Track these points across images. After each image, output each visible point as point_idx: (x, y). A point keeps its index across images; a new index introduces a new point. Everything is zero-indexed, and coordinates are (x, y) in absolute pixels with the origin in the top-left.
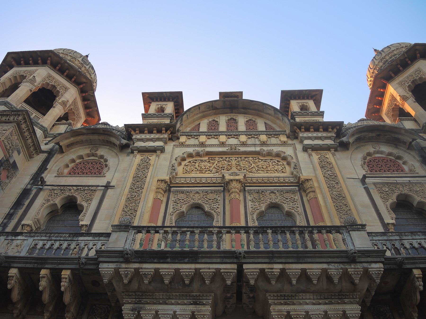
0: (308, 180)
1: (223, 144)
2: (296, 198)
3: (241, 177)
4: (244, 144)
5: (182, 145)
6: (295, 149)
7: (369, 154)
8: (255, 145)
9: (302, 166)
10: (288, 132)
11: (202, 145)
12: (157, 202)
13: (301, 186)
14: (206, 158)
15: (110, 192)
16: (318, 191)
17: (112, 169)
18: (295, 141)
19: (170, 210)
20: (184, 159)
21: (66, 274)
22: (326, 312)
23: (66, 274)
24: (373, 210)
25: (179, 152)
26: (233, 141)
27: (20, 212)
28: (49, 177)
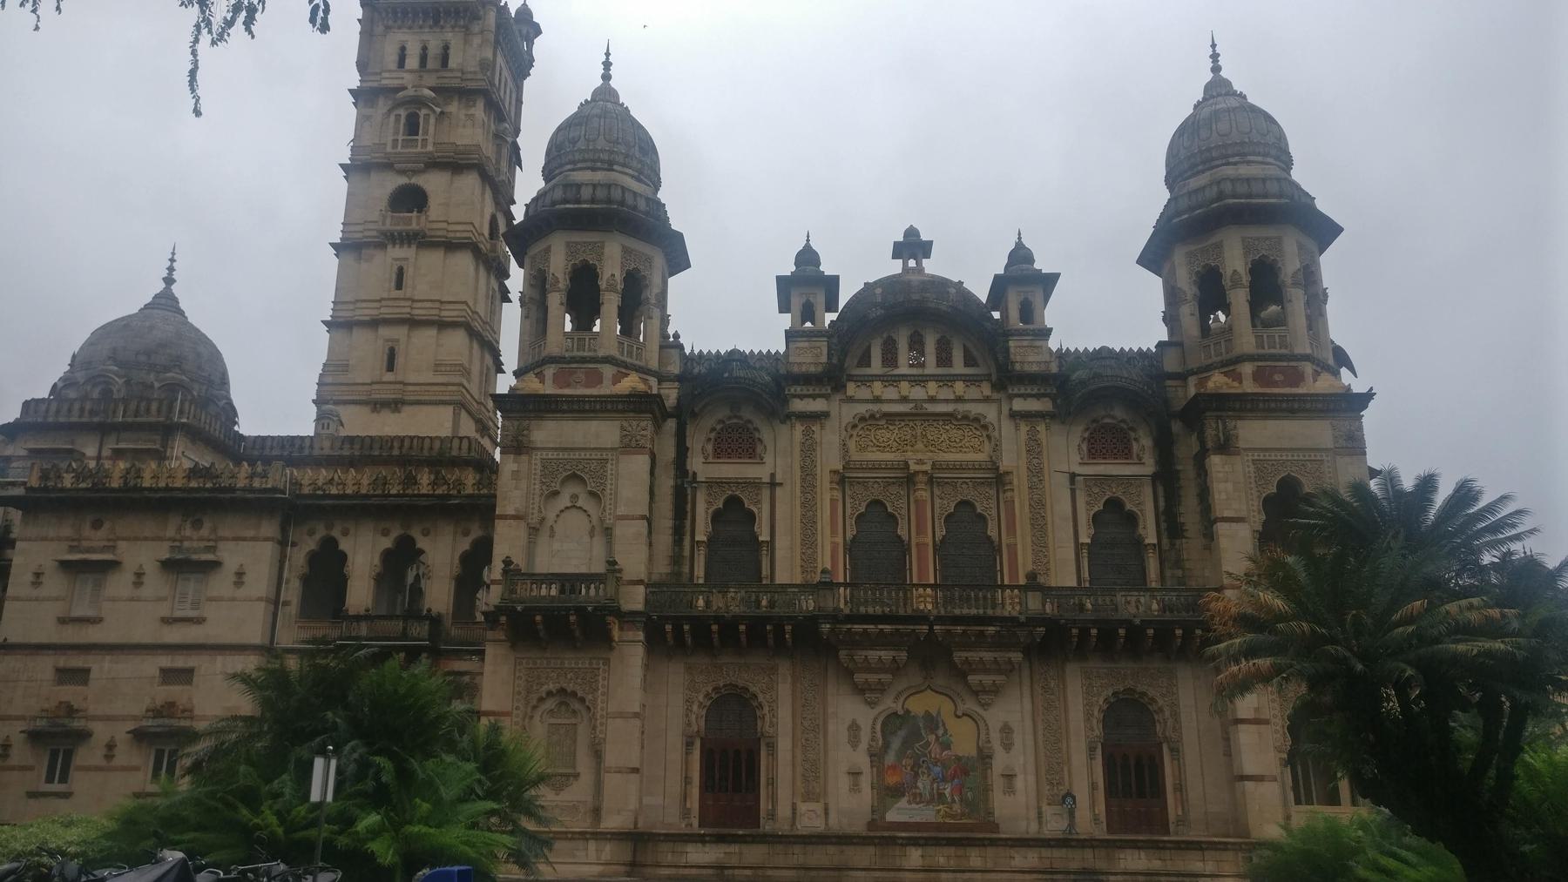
0: (1008, 473)
1: (904, 399)
3: (927, 467)
4: (932, 400)
5: (851, 400)
6: (1000, 412)
7: (1094, 421)
8: (947, 401)
9: (1004, 446)
10: (994, 378)
11: (877, 400)
13: (1000, 480)
14: (883, 422)
15: (778, 491)
17: (770, 448)
19: (848, 511)
20: (854, 426)
21: (788, 628)
23: (788, 628)
25: (849, 412)
26: (918, 393)
27: (688, 523)
28: (696, 464)
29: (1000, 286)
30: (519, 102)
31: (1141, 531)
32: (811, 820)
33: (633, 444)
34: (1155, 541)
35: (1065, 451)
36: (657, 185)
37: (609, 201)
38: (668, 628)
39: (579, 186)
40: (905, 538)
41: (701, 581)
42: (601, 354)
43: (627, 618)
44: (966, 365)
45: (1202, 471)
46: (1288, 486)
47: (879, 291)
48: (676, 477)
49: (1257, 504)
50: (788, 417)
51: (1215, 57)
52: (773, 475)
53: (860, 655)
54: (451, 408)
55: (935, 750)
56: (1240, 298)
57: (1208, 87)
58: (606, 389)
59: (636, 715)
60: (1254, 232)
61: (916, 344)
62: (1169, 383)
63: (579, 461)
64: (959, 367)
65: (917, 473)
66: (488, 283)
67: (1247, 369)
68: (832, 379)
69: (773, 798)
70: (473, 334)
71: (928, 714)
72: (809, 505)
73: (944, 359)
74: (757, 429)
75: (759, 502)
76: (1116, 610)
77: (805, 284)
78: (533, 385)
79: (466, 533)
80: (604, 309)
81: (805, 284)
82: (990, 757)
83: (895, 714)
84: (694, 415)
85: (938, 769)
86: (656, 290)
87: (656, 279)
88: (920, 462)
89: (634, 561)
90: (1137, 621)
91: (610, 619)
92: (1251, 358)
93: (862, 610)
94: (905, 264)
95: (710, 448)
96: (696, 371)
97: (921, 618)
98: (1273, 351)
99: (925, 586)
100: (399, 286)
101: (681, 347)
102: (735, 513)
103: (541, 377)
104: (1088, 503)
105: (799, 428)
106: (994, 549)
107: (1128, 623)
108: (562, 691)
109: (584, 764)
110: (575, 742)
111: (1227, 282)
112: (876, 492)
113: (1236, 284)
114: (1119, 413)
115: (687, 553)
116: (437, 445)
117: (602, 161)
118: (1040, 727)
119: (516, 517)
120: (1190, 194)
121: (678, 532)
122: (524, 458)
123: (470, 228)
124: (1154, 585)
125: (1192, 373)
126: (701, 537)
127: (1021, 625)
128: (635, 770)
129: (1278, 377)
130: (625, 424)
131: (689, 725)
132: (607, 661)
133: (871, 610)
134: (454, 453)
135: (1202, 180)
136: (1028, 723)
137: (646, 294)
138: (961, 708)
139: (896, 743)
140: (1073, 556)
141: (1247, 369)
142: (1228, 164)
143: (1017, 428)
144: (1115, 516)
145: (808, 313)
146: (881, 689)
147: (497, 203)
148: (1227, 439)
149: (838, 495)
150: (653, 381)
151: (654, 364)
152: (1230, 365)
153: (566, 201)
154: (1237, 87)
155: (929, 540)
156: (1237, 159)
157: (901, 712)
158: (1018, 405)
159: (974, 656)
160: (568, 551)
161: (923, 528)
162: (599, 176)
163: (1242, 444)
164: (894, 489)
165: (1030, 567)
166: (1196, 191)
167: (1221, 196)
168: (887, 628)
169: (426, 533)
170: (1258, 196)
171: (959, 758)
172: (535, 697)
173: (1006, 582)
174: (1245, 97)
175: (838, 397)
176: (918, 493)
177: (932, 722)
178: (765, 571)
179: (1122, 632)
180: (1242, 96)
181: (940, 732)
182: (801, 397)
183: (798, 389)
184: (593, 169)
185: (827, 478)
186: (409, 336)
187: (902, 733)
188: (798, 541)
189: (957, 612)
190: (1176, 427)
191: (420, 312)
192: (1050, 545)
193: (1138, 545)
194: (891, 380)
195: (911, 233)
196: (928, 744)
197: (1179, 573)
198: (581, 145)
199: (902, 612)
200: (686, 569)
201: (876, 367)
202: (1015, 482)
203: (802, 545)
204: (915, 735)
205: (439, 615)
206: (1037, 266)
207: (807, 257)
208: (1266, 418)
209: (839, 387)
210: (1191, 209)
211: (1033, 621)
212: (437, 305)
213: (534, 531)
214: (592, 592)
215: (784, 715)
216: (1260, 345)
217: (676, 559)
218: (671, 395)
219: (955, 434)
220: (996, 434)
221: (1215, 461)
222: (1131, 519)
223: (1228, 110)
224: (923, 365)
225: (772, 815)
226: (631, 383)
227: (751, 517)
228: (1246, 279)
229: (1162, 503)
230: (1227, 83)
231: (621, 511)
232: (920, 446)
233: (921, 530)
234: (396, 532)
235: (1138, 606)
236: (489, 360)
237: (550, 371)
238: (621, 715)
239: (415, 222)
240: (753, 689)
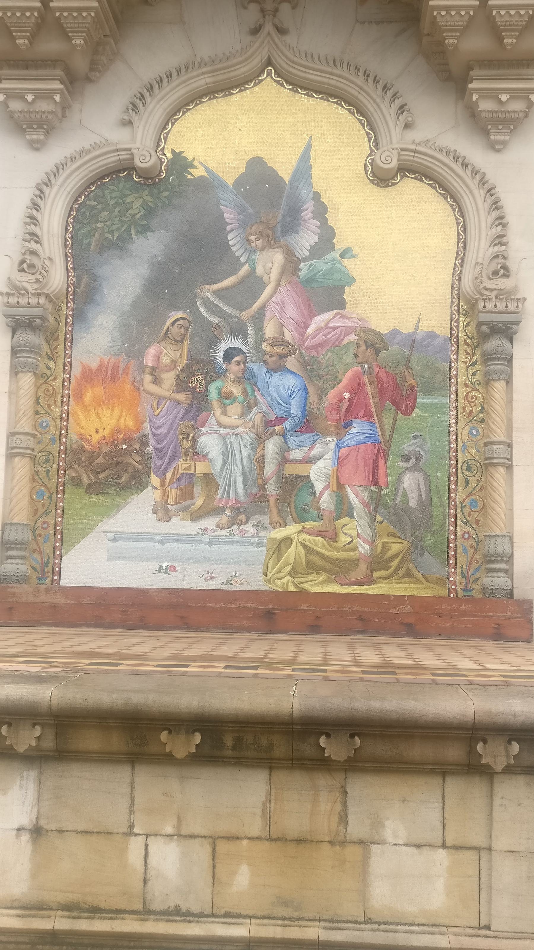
55: (280, 312)
71: (259, 178)
85: (284, 384)
139: (124, 281)
171: (373, 343)
181: (305, 240)
187: (150, 247)
196: (253, 285)
204: (200, 254)
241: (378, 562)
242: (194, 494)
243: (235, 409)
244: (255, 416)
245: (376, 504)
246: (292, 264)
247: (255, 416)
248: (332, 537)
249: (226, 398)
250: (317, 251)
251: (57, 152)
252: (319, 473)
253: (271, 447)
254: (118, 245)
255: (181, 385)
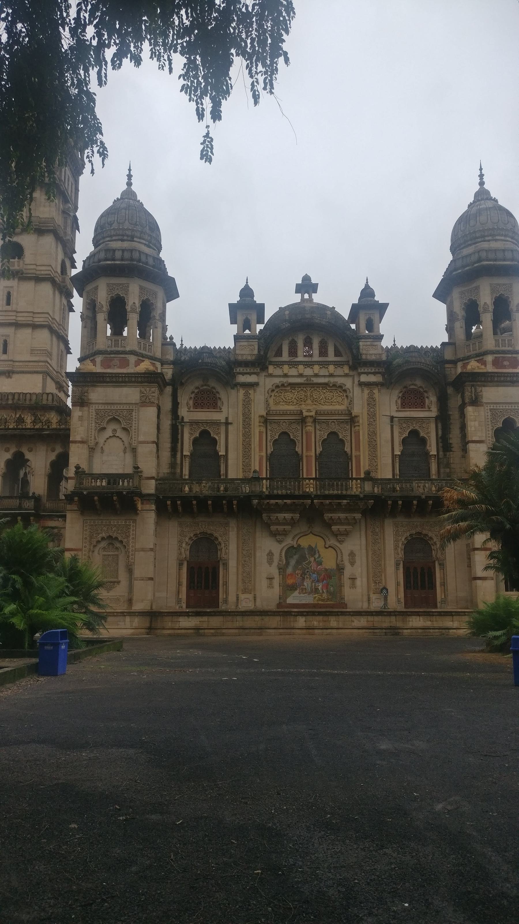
0: (356, 416)
1: (301, 375)
2: (347, 427)
3: (313, 414)
4: (316, 375)
5: (271, 375)
6: (354, 383)
7: (405, 387)
8: (324, 376)
10: (351, 363)
11: (286, 376)
12: (260, 433)
14: (289, 388)
15: (230, 426)
16: (361, 427)
17: (225, 403)
18: (355, 373)
19: (269, 438)
20: (273, 391)
21: (235, 502)
22: (347, 517)
23: (235, 502)
24: (390, 444)
26: (308, 372)
28: (183, 412)
29: (355, 310)
30: (77, 190)
31: (428, 448)
32: (246, 603)
33: (148, 400)
34: (436, 453)
35: (389, 403)
36: (159, 248)
37: (132, 259)
38: (169, 502)
39: (114, 251)
40: (300, 452)
41: (187, 477)
42: (128, 349)
43: (146, 498)
44: (336, 355)
45: (463, 415)
46: (508, 423)
47: (287, 312)
48: (172, 419)
49: (491, 433)
50: (236, 385)
51: (481, 176)
52: (227, 418)
53: (274, 516)
54: (40, 376)
55: (314, 565)
56: (487, 318)
57: (477, 195)
58: (131, 369)
59: (151, 550)
60: (497, 281)
61: (308, 343)
62: (447, 366)
63: (117, 410)
64: (331, 357)
65: (307, 416)
66: (61, 301)
67: (489, 358)
68: (260, 363)
69: (227, 592)
70: (52, 331)
71: (310, 547)
72: (247, 435)
73: (323, 352)
74: (218, 393)
75: (220, 433)
76: (412, 490)
77: (245, 308)
78: (90, 367)
79: (53, 450)
80: (129, 322)
81: (245, 308)
82: (343, 569)
83: (293, 547)
84: (182, 384)
85: (315, 575)
86: (159, 311)
87: (159, 304)
88: (309, 411)
89: (149, 466)
90: (423, 497)
91: (136, 498)
92: (492, 352)
93: (275, 492)
94: (302, 297)
95: (191, 403)
96: (183, 358)
97: (307, 496)
98: (504, 348)
99: (310, 479)
100: (8, 303)
101: (174, 345)
102: (205, 440)
103: (94, 362)
104: (400, 433)
105: (242, 392)
106: (348, 458)
107: (419, 498)
108: (110, 537)
109: (123, 576)
110: (117, 564)
111: (481, 309)
112: (284, 427)
113: (486, 311)
114: (419, 382)
115: (179, 461)
116: (34, 398)
117: (127, 236)
118: (370, 553)
119: (82, 442)
120: (463, 258)
121: (174, 450)
122: (86, 408)
123: (50, 268)
124: (434, 477)
125: (459, 360)
126: (186, 453)
127: (361, 499)
128: (151, 579)
129: (506, 363)
130: (143, 390)
131: (181, 554)
132: (135, 521)
133: (280, 492)
134: (44, 402)
135: (470, 250)
136: (364, 551)
137: (153, 314)
138: (328, 543)
139: (293, 562)
140: (390, 461)
141: (489, 358)
142: (484, 241)
143: (363, 391)
144: (414, 439)
145: (247, 325)
146: (285, 533)
147: (65, 253)
148: (476, 398)
149: (263, 429)
150: (158, 365)
151: (158, 355)
152: (480, 356)
153: (106, 259)
154: (493, 195)
155: (313, 454)
156: (490, 238)
157: (295, 546)
158: (364, 378)
159: (335, 516)
160: (112, 461)
161: (310, 448)
162: (126, 245)
163: (484, 400)
164: (294, 426)
165: (367, 468)
166: (466, 256)
167: (480, 260)
168: (288, 501)
169: (30, 450)
170: (500, 260)
171: (326, 570)
172: (94, 541)
173: (354, 476)
174: (496, 201)
175: (264, 374)
176: (308, 428)
177: (312, 551)
178: (223, 471)
179: (415, 502)
180: (496, 201)
181: (317, 556)
182: (243, 374)
183: (241, 369)
184: (122, 240)
185: (257, 419)
186: (15, 334)
187: (296, 557)
188: (241, 455)
189: (327, 492)
190: (450, 390)
191: (21, 319)
192: (378, 456)
193: (427, 454)
194: (293, 364)
195: (306, 279)
196: (310, 562)
197: (448, 470)
198: (115, 226)
199: (297, 493)
200: (178, 471)
201: (285, 356)
202: (361, 422)
203: (243, 457)
204: (303, 558)
205: (39, 496)
206: (376, 299)
207: (247, 292)
208: (498, 386)
209: (264, 368)
210: (463, 267)
211: (367, 497)
212: (31, 315)
213: (92, 450)
214: (126, 483)
215: (233, 547)
216: (497, 345)
217: (173, 465)
218: (168, 372)
219: (329, 395)
220: (351, 395)
221: (470, 410)
222: (423, 441)
223: (487, 209)
224: (311, 356)
225: (226, 601)
226: (145, 366)
227: (214, 442)
228: (491, 308)
229: (440, 433)
230: (488, 192)
231: (141, 438)
232: (309, 401)
233: (308, 449)
234: (13, 450)
235: (422, 489)
236: (62, 347)
237: (99, 359)
238: (143, 550)
239: (16, 264)
240: (216, 535)
241: (328, 599)
242: (303, 591)
243: (308, 579)
244: (311, 580)
245: (327, 592)
246: (315, 559)
247: (311, 580)
248: (322, 596)
249: (307, 578)
250: (318, 558)
251: (284, 544)
252: (320, 588)
253: (313, 584)
254: (292, 557)
255: (301, 576)
